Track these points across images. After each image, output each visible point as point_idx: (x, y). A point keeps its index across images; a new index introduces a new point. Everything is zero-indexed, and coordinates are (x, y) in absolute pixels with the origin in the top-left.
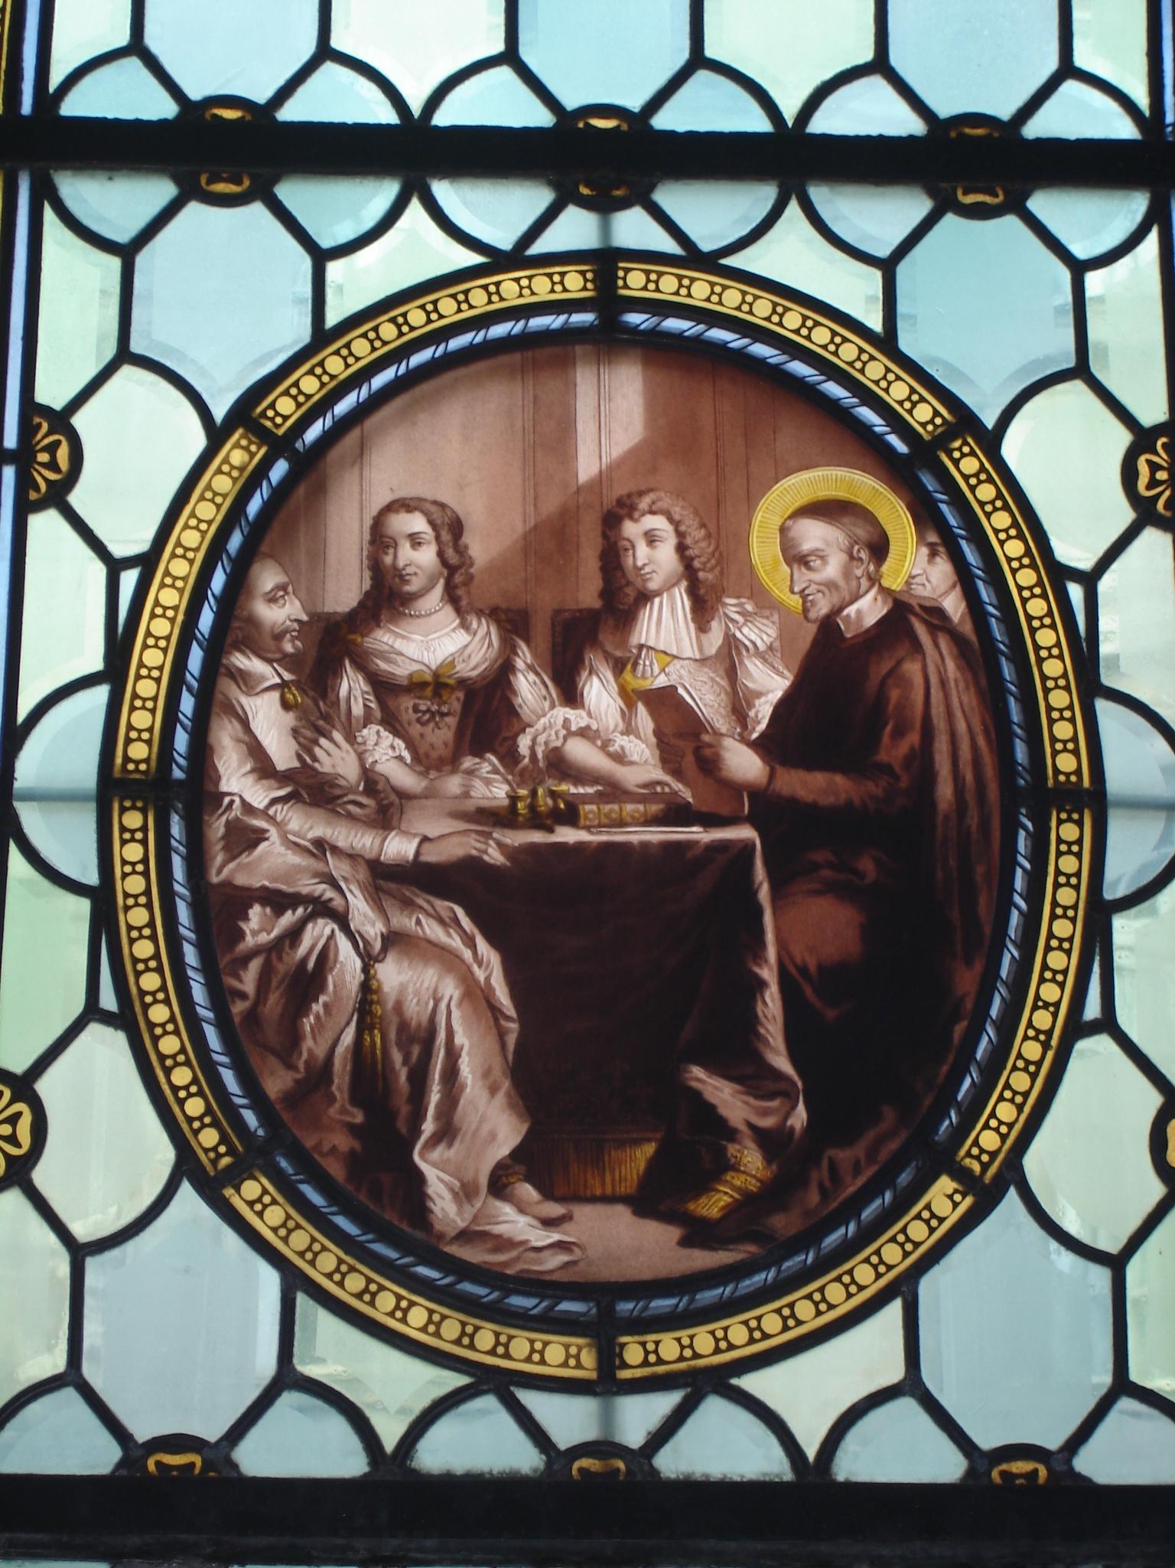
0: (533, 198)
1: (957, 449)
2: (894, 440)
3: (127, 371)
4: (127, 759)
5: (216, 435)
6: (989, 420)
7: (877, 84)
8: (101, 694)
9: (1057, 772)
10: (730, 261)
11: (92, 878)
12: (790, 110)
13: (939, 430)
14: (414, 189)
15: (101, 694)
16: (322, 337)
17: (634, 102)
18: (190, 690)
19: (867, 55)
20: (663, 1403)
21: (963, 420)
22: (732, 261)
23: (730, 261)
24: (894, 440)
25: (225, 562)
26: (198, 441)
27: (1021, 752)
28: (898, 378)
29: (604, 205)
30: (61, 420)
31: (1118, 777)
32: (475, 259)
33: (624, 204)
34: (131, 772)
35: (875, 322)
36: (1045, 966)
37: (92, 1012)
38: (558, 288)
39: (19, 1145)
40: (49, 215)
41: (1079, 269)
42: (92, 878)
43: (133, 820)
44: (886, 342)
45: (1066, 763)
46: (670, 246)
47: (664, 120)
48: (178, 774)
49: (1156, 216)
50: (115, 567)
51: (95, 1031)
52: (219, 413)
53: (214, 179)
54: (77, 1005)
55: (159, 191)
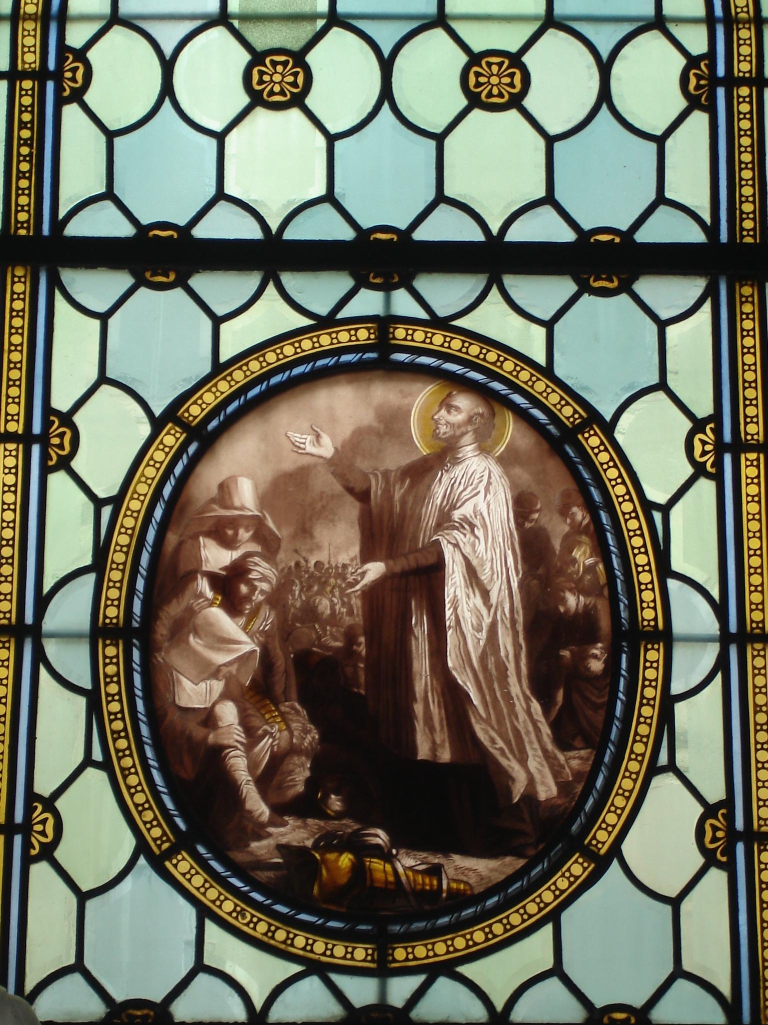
0: (342, 283)
2: (551, 428)
3: (105, 389)
4: (105, 617)
5: (158, 424)
7: (548, 211)
8: (91, 578)
10: (457, 323)
11: (86, 683)
12: (495, 229)
14: (271, 276)
15: (91, 578)
17: (402, 224)
18: (142, 576)
19: (541, 193)
20: (414, 982)
21: (593, 417)
23: (457, 323)
24: (551, 428)
25: (162, 503)
26: (146, 430)
28: (553, 391)
30: (67, 419)
31: (679, 626)
32: (306, 322)
33: (396, 287)
34: (108, 624)
35: (541, 359)
36: (636, 733)
37: (88, 762)
39: (47, 837)
40: (58, 297)
41: (662, 325)
42: (86, 683)
43: (111, 651)
46: (423, 315)
47: (421, 234)
49: (711, 292)
50: (98, 503)
51: (90, 771)
52: (158, 412)
53: (154, 274)
54: (79, 757)
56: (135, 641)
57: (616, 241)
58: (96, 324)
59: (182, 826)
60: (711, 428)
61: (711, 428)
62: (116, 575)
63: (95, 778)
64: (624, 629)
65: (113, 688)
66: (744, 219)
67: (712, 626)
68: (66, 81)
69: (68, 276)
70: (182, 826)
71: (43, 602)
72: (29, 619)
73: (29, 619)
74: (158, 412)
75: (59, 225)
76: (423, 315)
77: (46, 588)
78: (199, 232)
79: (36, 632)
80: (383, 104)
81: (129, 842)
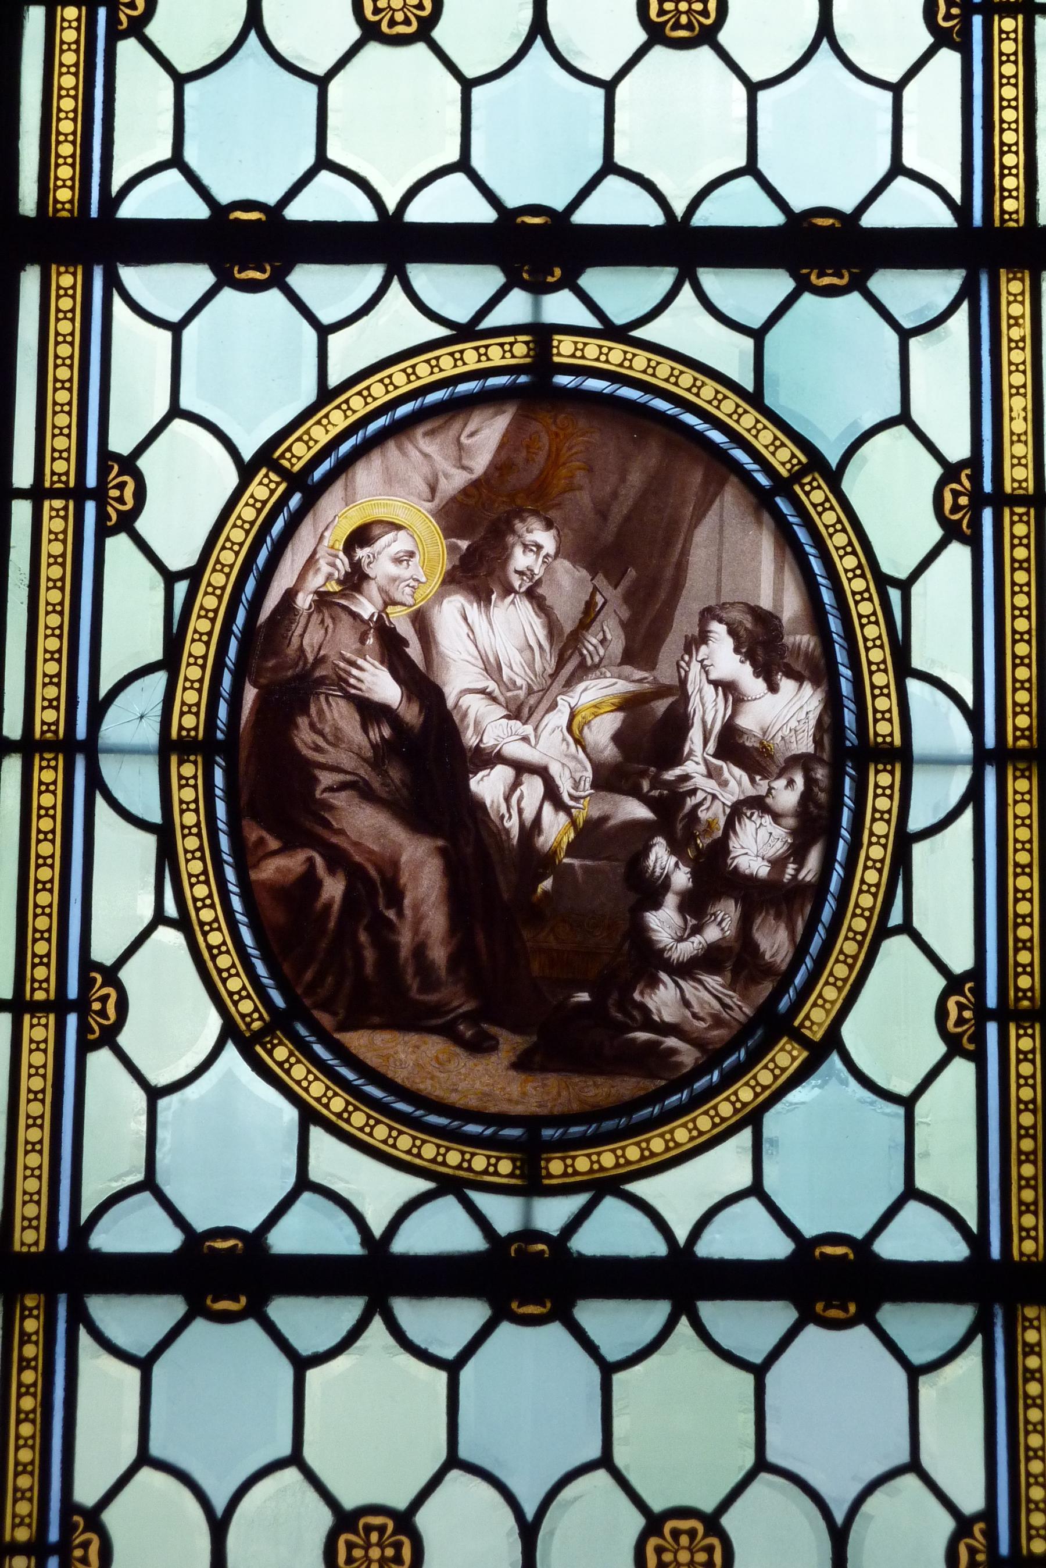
1: (807, 484)
5: (247, 471)
6: (833, 461)
9: (876, 734)
11: (155, 816)
13: (796, 468)
16: (326, 395)
22: (638, 333)
23: (637, 333)
26: (232, 479)
27: (849, 718)
29: (539, 288)
38: (508, 355)
42: (155, 816)
44: (755, 399)
45: (883, 728)
48: (220, 735)
52: (247, 455)
55: (201, 277)
56: (218, 759)
57: (836, 226)
58: (167, 336)
59: (279, 1001)
60: (967, 475)
61: (967, 475)
62: (194, 673)
63: (169, 938)
64: (848, 744)
65: (190, 819)
66: (1005, 198)
67: (962, 739)
68: (122, 7)
69: (129, 275)
70: (279, 1001)
71: (98, 709)
72: (81, 731)
73: (81, 731)
74: (247, 455)
75: (111, 202)
76: (591, 321)
77: (104, 690)
78: (294, 212)
79: (91, 748)
80: (535, 39)
81: (214, 1023)
